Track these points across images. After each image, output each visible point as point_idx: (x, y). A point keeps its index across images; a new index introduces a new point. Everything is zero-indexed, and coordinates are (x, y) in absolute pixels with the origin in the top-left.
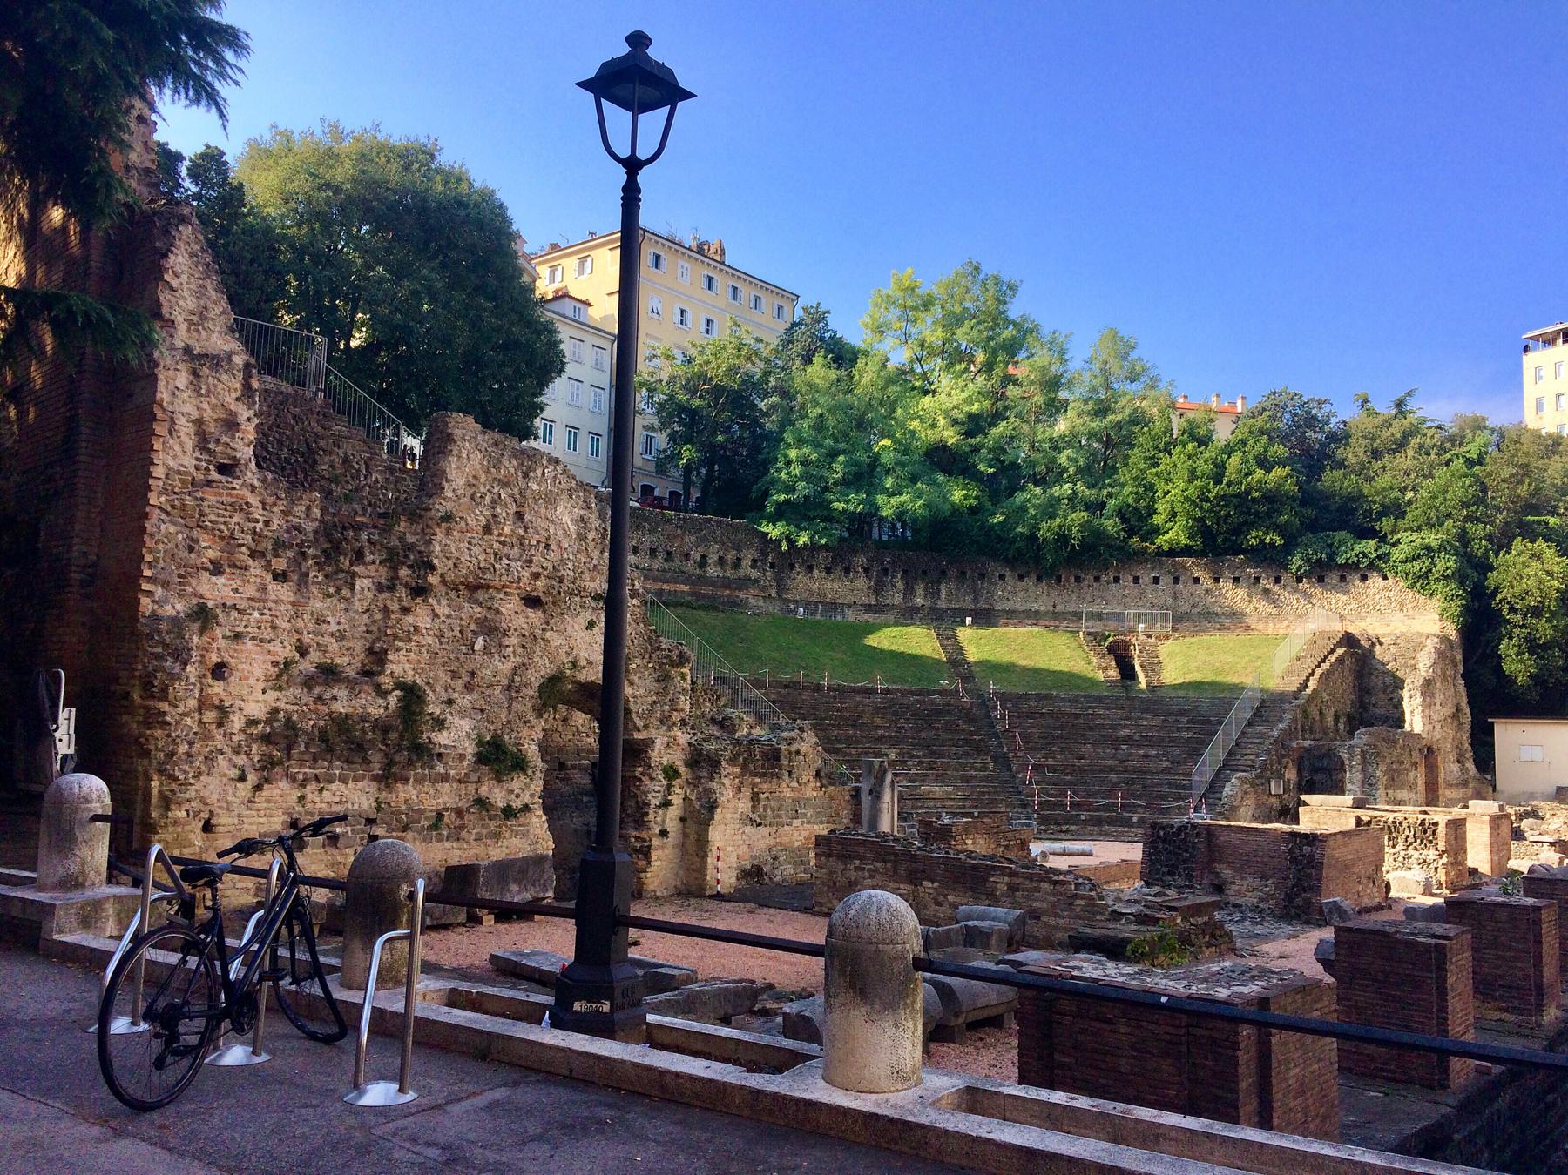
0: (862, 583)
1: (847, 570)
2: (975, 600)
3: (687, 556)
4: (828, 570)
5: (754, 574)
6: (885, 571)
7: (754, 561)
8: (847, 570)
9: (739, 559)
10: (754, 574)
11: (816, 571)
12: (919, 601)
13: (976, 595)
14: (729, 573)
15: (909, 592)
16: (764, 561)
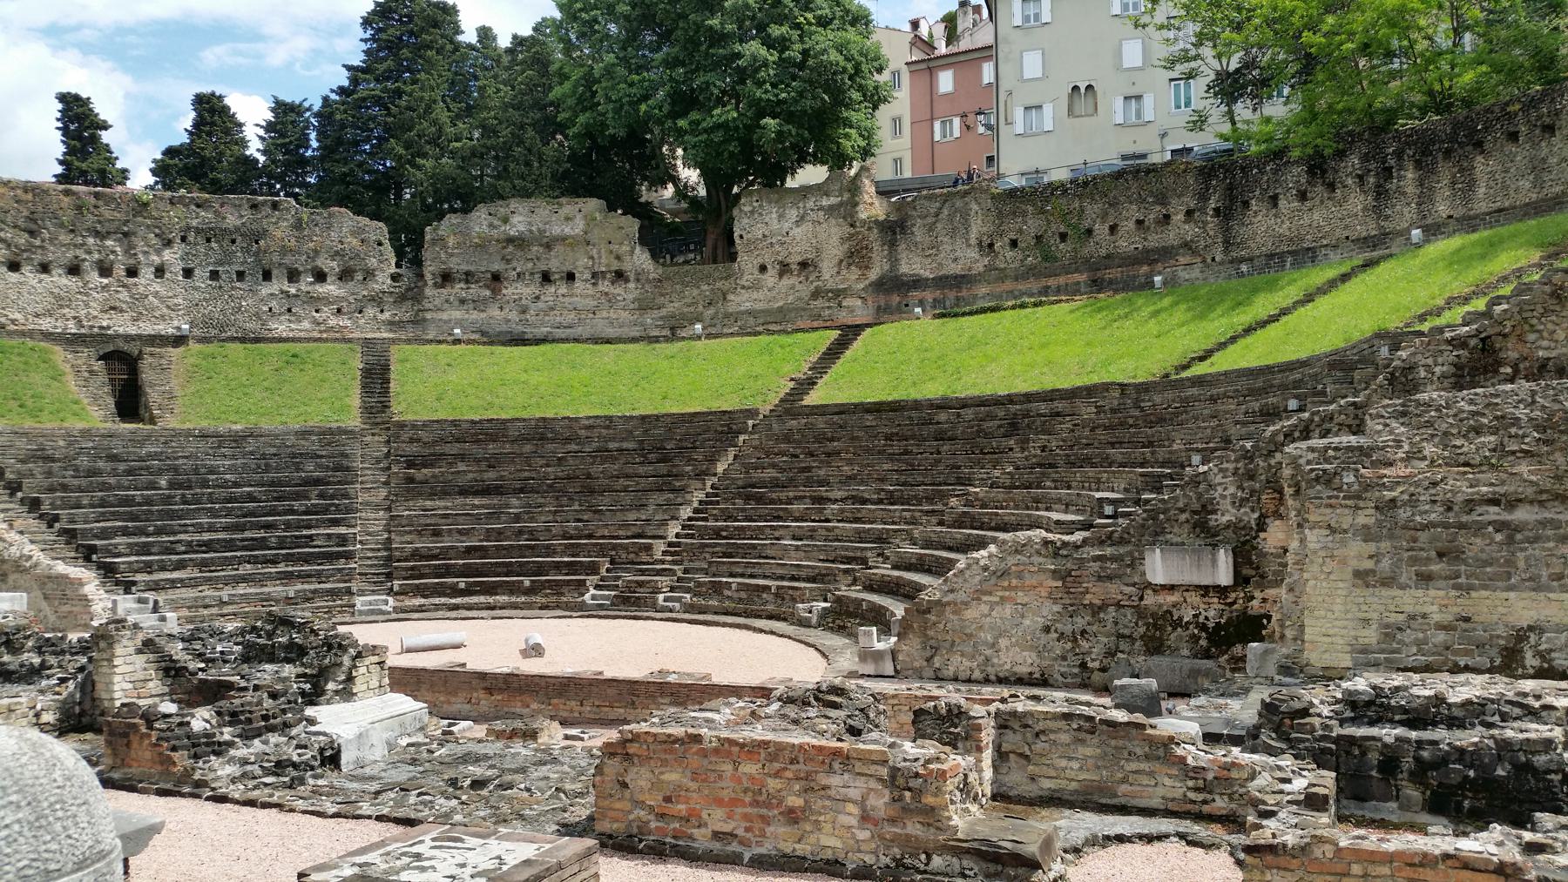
0: (1357, 202)
1: (1331, 187)
2: (1538, 184)
3: (1089, 232)
4: (1303, 196)
5: (1190, 231)
6: (1387, 173)
7: (1189, 213)
8: (1331, 187)
9: (1167, 217)
10: (1190, 231)
11: (1282, 203)
12: (1442, 209)
13: (1538, 168)
14: (1154, 240)
15: (1425, 198)
16: (1203, 211)
